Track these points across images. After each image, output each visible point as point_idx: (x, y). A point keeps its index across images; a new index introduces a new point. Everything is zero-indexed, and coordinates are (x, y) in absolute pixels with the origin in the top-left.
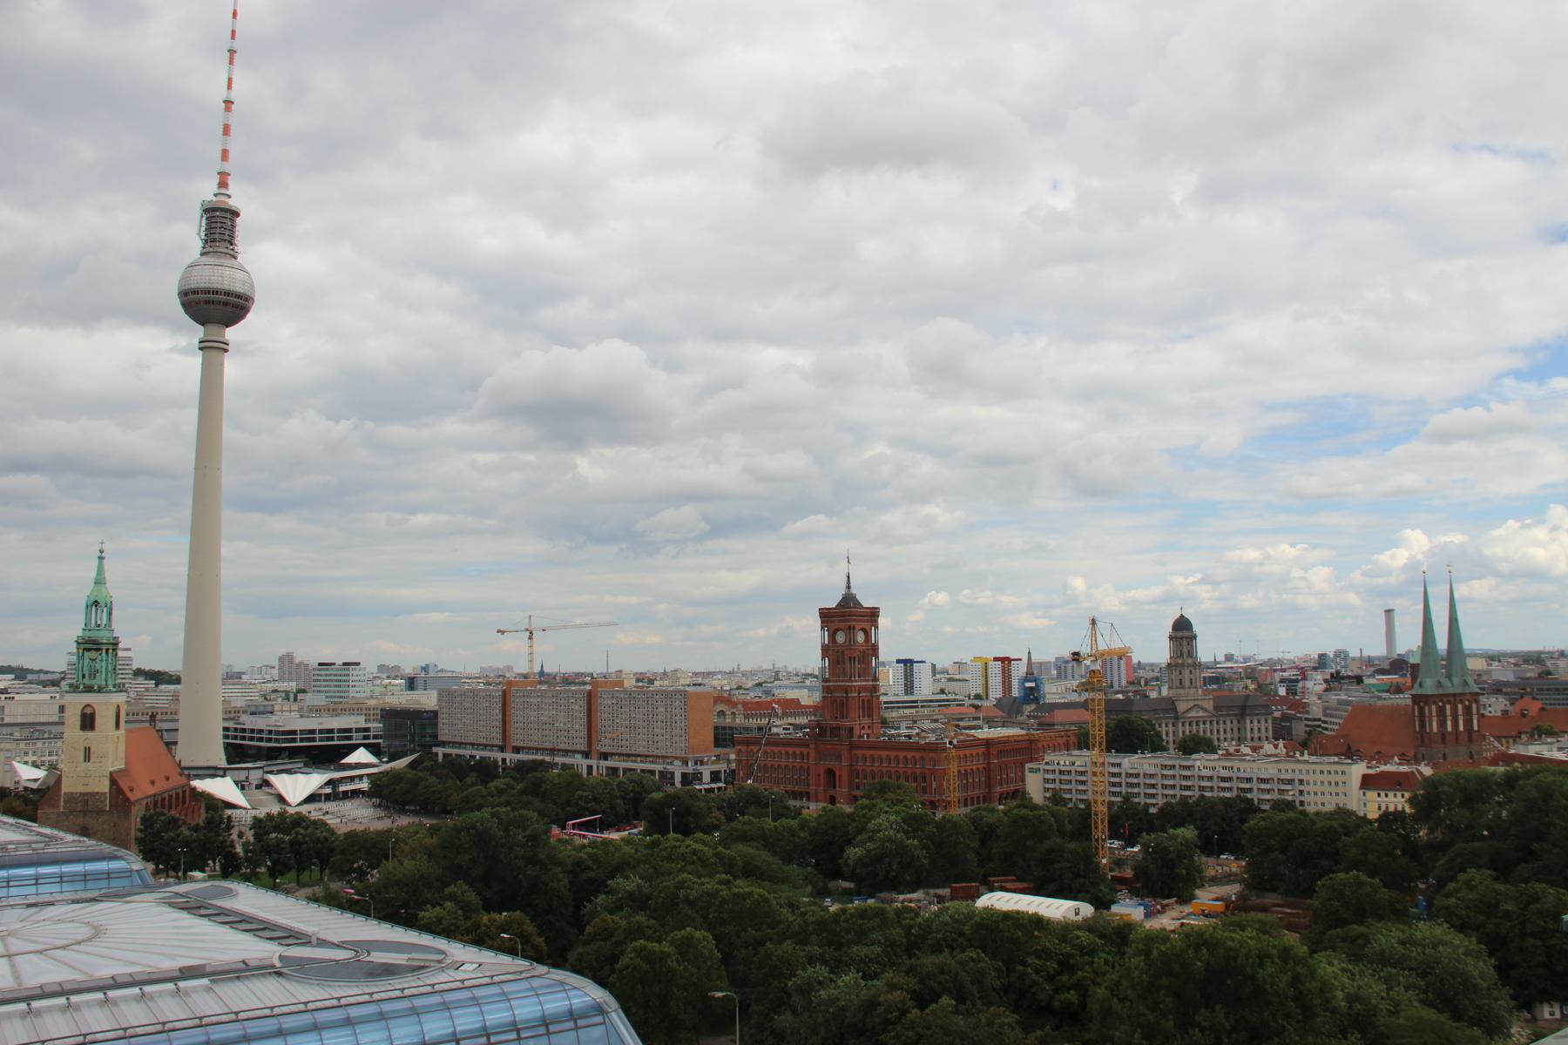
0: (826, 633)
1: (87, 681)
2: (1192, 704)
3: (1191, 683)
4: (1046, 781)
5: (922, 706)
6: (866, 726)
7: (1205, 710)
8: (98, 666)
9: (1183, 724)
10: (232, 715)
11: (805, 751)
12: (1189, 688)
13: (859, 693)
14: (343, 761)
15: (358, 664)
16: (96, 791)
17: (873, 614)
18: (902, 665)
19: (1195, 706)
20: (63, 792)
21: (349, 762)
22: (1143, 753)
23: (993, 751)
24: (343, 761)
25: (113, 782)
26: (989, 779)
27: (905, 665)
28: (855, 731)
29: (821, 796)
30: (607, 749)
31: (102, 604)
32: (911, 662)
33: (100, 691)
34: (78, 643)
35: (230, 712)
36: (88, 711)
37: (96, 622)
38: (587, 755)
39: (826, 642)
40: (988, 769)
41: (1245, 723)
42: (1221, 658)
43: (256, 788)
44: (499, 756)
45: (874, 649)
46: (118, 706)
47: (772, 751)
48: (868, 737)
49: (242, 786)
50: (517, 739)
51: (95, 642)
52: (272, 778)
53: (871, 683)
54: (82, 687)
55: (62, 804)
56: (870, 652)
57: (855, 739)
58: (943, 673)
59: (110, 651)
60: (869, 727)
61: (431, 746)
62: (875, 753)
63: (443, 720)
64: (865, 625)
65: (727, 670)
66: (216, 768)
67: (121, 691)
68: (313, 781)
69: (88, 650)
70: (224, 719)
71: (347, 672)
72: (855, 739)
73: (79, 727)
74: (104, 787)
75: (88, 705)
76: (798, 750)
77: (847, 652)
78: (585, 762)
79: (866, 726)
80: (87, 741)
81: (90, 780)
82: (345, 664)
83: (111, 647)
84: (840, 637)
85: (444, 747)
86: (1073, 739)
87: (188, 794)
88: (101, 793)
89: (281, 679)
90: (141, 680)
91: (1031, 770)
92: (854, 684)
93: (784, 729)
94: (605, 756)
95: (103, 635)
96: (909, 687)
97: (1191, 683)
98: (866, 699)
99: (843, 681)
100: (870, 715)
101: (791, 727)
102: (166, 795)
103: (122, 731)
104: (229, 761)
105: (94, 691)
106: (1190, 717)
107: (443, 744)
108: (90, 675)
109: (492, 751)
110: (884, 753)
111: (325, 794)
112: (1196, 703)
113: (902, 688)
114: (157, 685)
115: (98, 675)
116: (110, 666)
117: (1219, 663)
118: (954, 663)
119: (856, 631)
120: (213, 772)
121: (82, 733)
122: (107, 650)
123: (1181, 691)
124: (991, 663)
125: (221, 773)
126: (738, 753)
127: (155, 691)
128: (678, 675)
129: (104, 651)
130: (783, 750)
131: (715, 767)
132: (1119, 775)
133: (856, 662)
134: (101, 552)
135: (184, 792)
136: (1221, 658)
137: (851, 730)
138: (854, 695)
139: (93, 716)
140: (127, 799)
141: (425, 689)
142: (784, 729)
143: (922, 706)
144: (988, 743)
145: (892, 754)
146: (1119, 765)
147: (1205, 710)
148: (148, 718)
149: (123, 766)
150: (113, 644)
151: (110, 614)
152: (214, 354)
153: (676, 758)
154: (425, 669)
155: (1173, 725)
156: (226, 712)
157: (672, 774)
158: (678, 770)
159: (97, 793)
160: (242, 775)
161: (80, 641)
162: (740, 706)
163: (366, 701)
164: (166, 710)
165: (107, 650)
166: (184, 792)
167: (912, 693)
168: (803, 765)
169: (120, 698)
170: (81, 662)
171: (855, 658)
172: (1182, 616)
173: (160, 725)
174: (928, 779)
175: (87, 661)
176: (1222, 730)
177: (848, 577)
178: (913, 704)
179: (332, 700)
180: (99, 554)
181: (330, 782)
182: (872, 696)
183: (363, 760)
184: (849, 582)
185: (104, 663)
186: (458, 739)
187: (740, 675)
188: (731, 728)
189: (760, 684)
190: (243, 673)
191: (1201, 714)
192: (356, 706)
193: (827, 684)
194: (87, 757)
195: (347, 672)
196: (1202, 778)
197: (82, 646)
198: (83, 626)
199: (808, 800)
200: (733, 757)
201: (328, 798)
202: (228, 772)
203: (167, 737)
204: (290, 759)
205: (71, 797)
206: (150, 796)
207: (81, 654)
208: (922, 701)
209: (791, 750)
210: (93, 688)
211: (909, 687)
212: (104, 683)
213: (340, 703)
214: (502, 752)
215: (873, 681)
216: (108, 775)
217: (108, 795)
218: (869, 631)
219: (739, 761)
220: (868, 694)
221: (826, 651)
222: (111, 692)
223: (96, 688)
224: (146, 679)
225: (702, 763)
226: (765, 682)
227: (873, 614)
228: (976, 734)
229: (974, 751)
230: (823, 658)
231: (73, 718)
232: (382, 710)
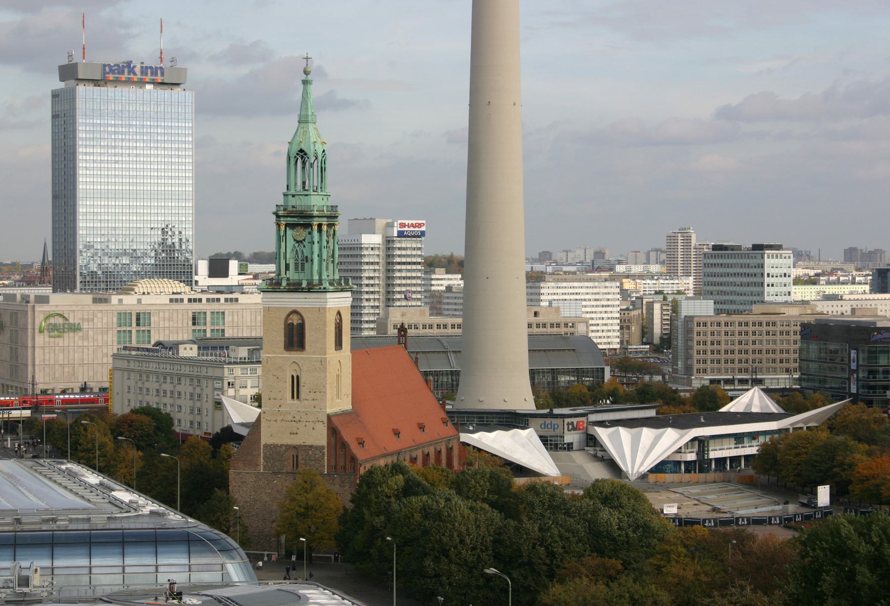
14: (724, 409)
16: (309, 443)
20: (263, 442)
21: (732, 410)
24: (724, 409)
25: (333, 431)
34: (278, 216)
36: (295, 320)
37: (304, 183)
46: (339, 313)
49: (551, 443)
54: (284, 283)
59: (325, 228)
69: (292, 226)
73: (282, 345)
74: (319, 437)
75: (295, 312)
83: (324, 221)
87: (456, 452)
102: (419, 454)
105: (302, 290)
108: (296, 265)
111: (686, 462)
115: (307, 265)
116: (325, 252)
121: (287, 355)
122: (320, 226)
129: (315, 228)
135: (450, 450)
139: (302, 326)
149: (349, 407)
150: (327, 217)
151: (323, 170)
159: (311, 447)
163: (783, 310)
165: (320, 226)
166: (450, 450)
170: (283, 244)
175: (291, 243)
180: (304, 77)
185: (316, 247)
192: (765, 319)
194: (296, 392)
198: (285, 190)
202: (532, 421)
204: (642, 403)
205: (275, 451)
206: (391, 454)
207: (282, 233)
210: (301, 284)
212: (316, 277)
216: (326, 421)
217: (326, 451)
223: (304, 285)
224: (447, 272)
232: (803, 325)
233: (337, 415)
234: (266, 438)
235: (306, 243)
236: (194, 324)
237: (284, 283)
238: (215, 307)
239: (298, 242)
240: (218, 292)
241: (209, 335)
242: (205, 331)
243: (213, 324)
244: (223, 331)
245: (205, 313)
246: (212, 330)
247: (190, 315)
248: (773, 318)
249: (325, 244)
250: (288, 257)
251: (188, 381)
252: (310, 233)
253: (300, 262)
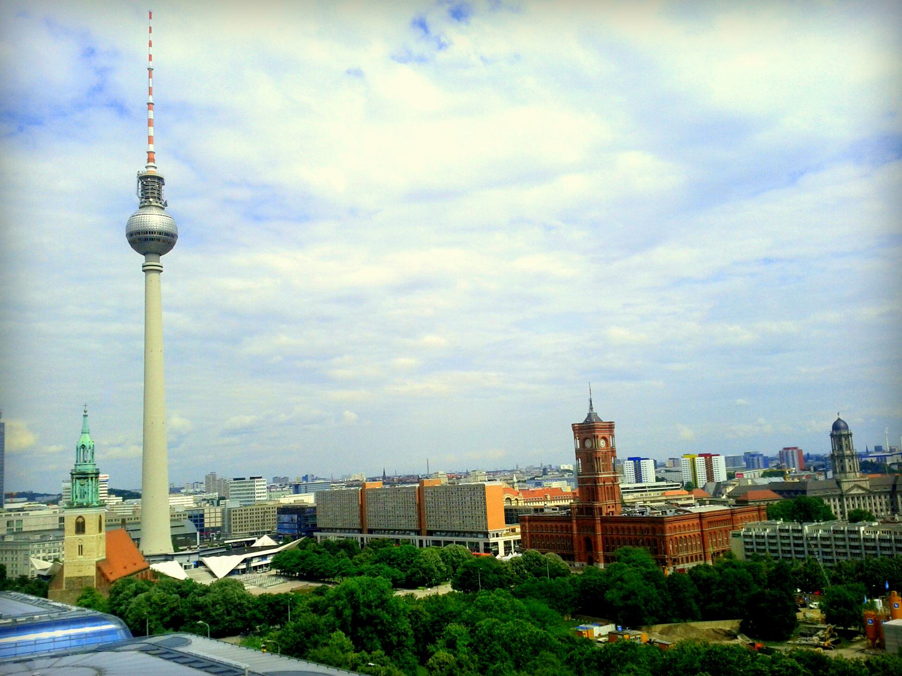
0: (578, 441)
1: (79, 500)
2: (852, 484)
3: (851, 469)
4: (746, 543)
5: (649, 491)
6: (611, 506)
7: (863, 488)
8: (86, 490)
9: (847, 499)
10: (176, 518)
11: (569, 525)
12: (849, 472)
13: (604, 483)
14: (252, 546)
15: (261, 477)
16: (87, 575)
17: (610, 427)
18: (632, 461)
19: (855, 485)
20: (65, 577)
22: (818, 521)
23: (704, 522)
24: (253, 546)
25: (99, 569)
26: (703, 543)
27: (635, 462)
28: (603, 510)
29: (582, 557)
30: (433, 528)
31: (88, 447)
32: (639, 459)
33: (87, 506)
34: (72, 475)
35: (174, 516)
36: (80, 520)
38: (418, 533)
39: (579, 447)
40: (702, 536)
41: (896, 498)
42: (871, 448)
43: (195, 567)
44: (359, 536)
45: (613, 451)
46: (100, 516)
47: (546, 526)
48: (613, 514)
50: (371, 524)
51: (83, 473)
52: (206, 560)
53: (612, 475)
55: (64, 585)
56: (610, 453)
57: (604, 515)
58: (662, 466)
59: (94, 479)
60: (613, 507)
61: (312, 531)
62: (620, 525)
63: (319, 513)
64: (606, 435)
65: (509, 469)
66: (167, 555)
67: (102, 506)
68: (234, 561)
70: (171, 520)
71: (252, 484)
72: (604, 515)
74: (92, 572)
75: (80, 517)
76: (564, 524)
77: (594, 454)
78: (417, 538)
79: (611, 506)
80: (80, 541)
81: (83, 567)
82: (251, 478)
83: (94, 475)
84: (588, 444)
85: (321, 532)
86: (764, 513)
88: (90, 577)
89: (208, 491)
90: (113, 497)
91: (734, 535)
92: (600, 476)
93: (553, 509)
94: (430, 533)
95: (89, 468)
96: (639, 479)
97: (851, 469)
98: (609, 487)
99: (593, 475)
100: (614, 498)
101: (558, 508)
103: (103, 533)
104: (175, 552)
106: (851, 494)
107: (320, 530)
109: (354, 533)
110: (626, 525)
111: (241, 569)
112: (856, 483)
113: (633, 479)
114: (124, 500)
117: (870, 453)
118: (670, 459)
119: (599, 439)
120: (167, 558)
122: (92, 478)
123: (843, 475)
124: (698, 459)
125: (170, 558)
126: (522, 528)
127: (122, 504)
128: (477, 474)
130: (553, 524)
131: (507, 538)
132: (801, 538)
133: (601, 461)
134: (85, 412)
136: (871, 448)
137: (601, 509)
138: (601, 484)
140: (108, 580)
141: (306, 492)
142: (553, 509)
143: (649, 491)
144: (701, 516)
145: (631, 525)
146: (801, 531)
147: (863, 488)
148: (120, 522)
149: (104, 557)
152: (154, 276)
153: (480, 533)
154: (305, 478)
155: (839, 500)
156: (172, 516)
157: (478, 543)
158: (481, 541)
159: (88, 576)
160: (184, 560)
161: (74, 473)
162: (521, 495)
163: (267, 503)
164: (131, 517)
165: (92, 478)
167: (641, 482)
168: (568, 535)
169: (102, 511)
170: (74, 487)
171: (599, 458)
172: (839, 419)
173: (130, 527)
174: (658, 543)
175: (78, 486)
176: (878, 503)
177: (591, 401)
178: (642, 490)
179: (244, 503)
180: (84, 414)
181: (245, 561)
182: (614, 485)
183: (266, 545)
184: (591, 405)
186: (330, 526)
187: (519, 472)
188: (516, 510)
189: (533, 479)
190: (182, 488)
191: (860, 491)
192: (260, 507)
193: (581, 477)
195: (252, 484)
196: (866, 540)
197: (75, 476)
198: (75, 463)
199: (574, 560)
200: (518, 530)
201: (244, 571)
202: (175, 558)
203: (135, 535)
205: (71, 581)
208: (649, 487)
209: (559, 524)
211: (639, 479)
212: (90, 501)
213: (249, 505)
214: (361, 533)
215: (613, 473)
216: (95, 563)
218: (608, 439)
219: (523, 534)
220: (611, 483)
221: (578, 452)
222: (95, 507)
224: (116, 496)
225: (497, 536)
226: (537, 477)
227: (610, 427)
228: (690, 510)
229: (690, 522)
230: (577, 459)
231: (70, 526)
232: (278, 508)
233: (99, 561)
234: (68, 573)
235: (85, 486)
236: (8, 526)
237: (75, 504)
238: (18, 518)
239: (82, 485)
240: (18, 511)
241: (15, 531)
242: (13, 529)
243: (17, 526)
244: (22, 528)
245: (13, 521)
246: (17, 529)
247: (6, 522)
248: (263, 506)
249: (94, 485)
250: (77, 492)
251: (11, 552)
252: (88, 481)
253: (82, 494)
